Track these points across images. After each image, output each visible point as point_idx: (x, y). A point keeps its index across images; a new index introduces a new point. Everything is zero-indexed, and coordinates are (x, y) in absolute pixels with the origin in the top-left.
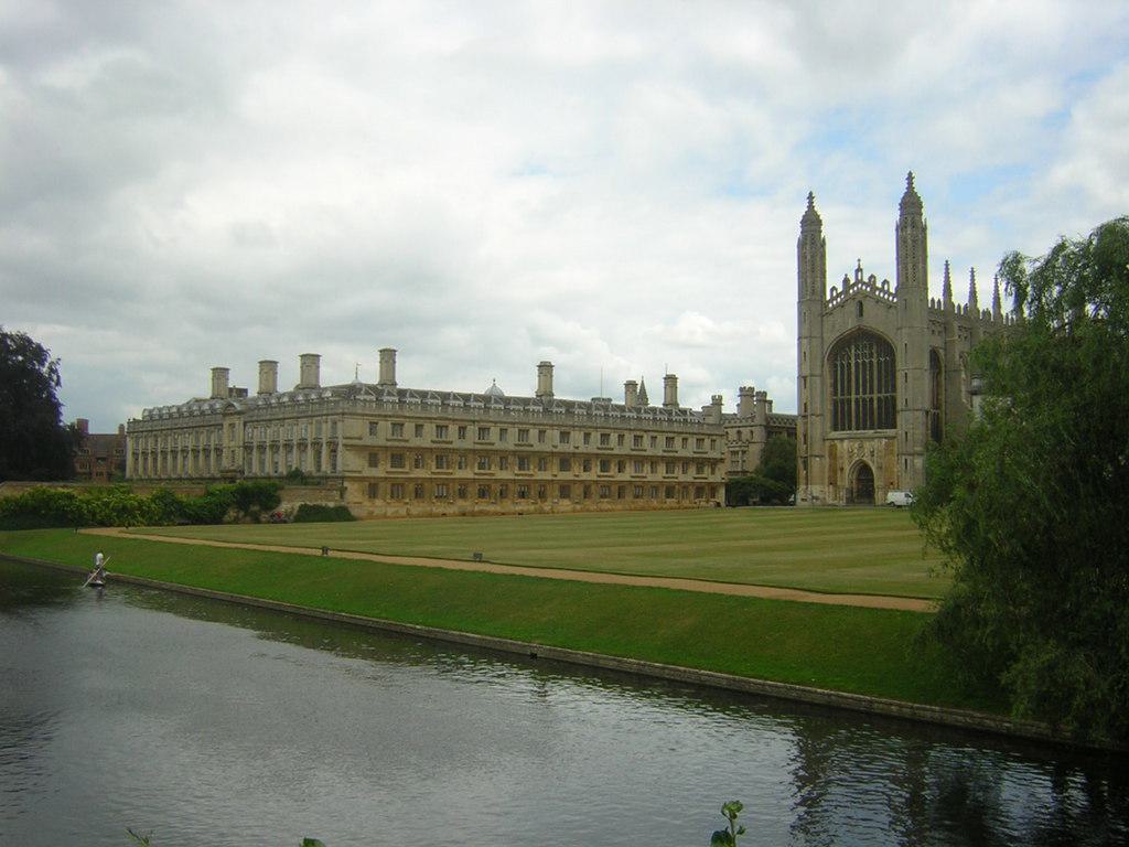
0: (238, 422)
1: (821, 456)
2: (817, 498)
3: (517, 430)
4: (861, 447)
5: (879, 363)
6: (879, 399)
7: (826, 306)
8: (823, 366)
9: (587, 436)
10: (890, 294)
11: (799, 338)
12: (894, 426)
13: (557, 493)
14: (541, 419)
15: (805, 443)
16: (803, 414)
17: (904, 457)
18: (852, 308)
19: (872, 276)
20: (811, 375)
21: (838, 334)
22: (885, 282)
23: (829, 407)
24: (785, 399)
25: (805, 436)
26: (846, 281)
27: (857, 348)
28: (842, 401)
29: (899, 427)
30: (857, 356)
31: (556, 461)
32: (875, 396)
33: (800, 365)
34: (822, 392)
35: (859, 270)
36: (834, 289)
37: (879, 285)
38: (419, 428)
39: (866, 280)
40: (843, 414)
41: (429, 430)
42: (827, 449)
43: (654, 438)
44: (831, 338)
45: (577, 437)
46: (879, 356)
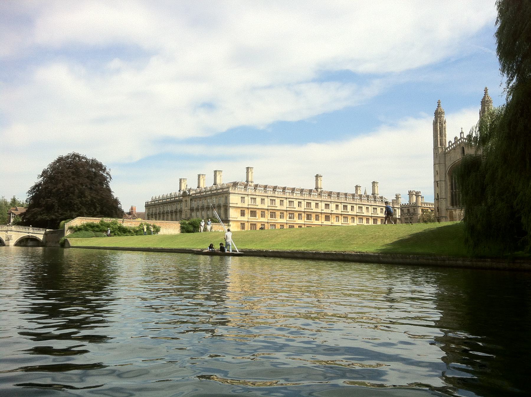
0: (188, 199)
3: (305, 202)
8: (446, 177)
9: (337, 206)
11: (434, 165)
14: (316, 198)
15: (438, 212)
18: (459, 151)
21: (452, 162)
23: (449, 195)
26: (456, 138)
31: (324, 216)
33: (435, 176)
38: (263, 200)
39: (465, 137)
41: (267, 201)
42: (448, 213)
43: (367, 208)
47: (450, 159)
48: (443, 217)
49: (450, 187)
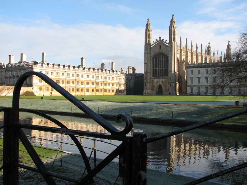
1: (150, 83)
2: (148, 93)
4: (160, 80)
5: (164, 60)
6: (164, 69)
7: (151, 46)
10: (167, 44)
11: (145, 54)
12: (167, 75)
13: (86, 90)
15: (146, 79)
16: (145, 72)
17: (170, 83)
18: (158, 47)
19: (163, 39)
20: (148, 63)
22: (166, 41)
23: (152, 71)
24: (140, 70)
25: (146, 78)
26: (156, 40)
27: (159, 57)
28: (155, 69)
29: (169, 76)
30: (159, 59)
31: (86, 82)
32: (163, 68)
33: (145, 60)
34: (150, 67)
35: (160, 37)
36: (153, 42)
37: (165, 41)
39: (162, 40)
40: (155, 72)
44: (153, 54)
45: (91, 76)
46: (164, 59)
47: (153, 51)
48: (148, 83)
49: (153, 66)
